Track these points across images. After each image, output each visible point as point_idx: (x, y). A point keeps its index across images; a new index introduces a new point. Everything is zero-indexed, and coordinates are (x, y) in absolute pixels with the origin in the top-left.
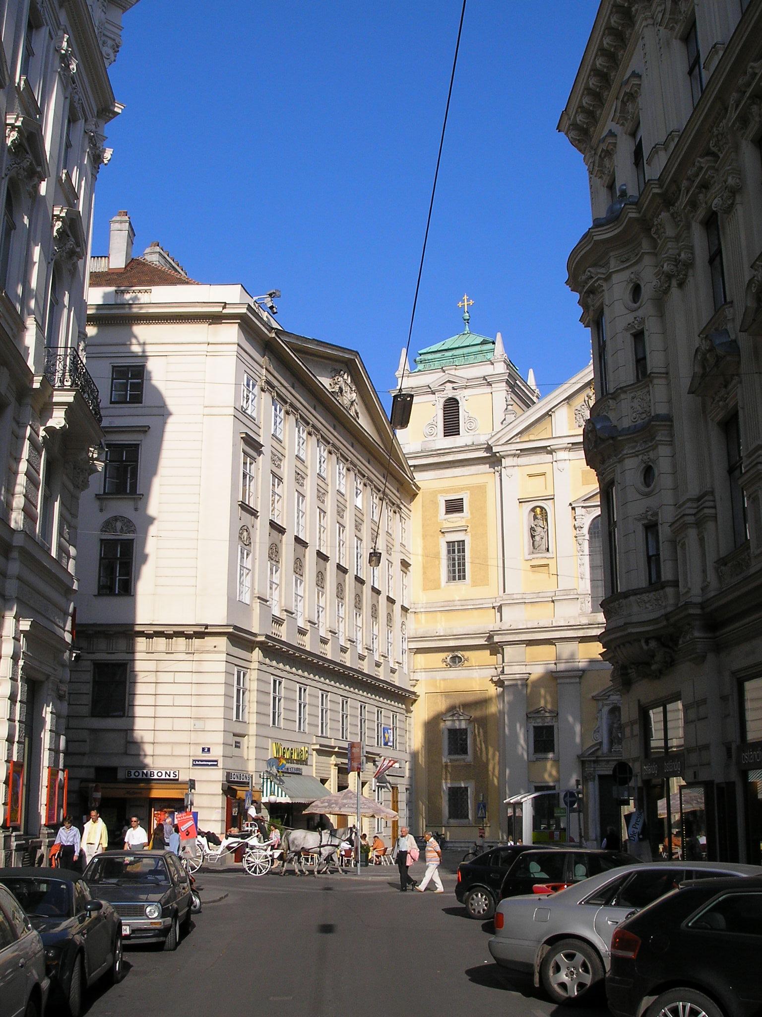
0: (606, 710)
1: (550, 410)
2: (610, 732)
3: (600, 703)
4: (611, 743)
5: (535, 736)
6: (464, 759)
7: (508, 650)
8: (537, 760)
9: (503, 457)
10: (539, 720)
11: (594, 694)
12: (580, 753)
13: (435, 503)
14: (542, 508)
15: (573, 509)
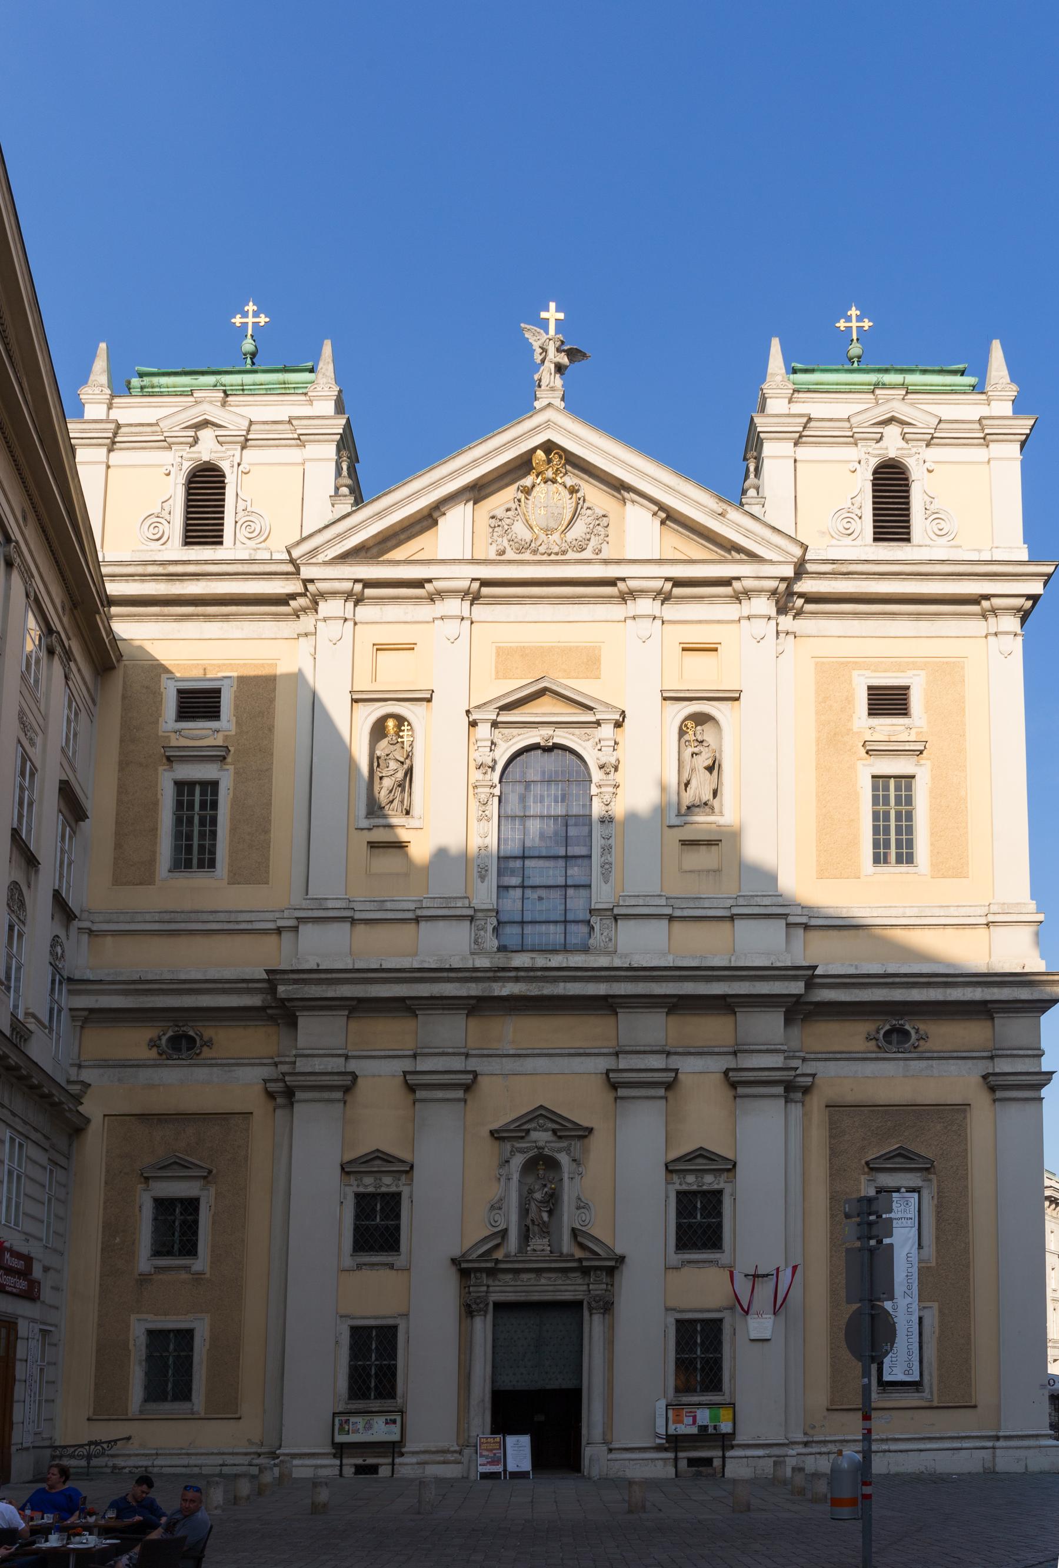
0: (518, 1160)
2: (524, 1212)
3: (508, 1146)
4: (525, 1236)
5: (357, 1217)
6: (187, 1268)
7: (305, 1022)
8: (360, 1267)
10: (368, 1180)
11: (495, 1126)
12: (457, 1253)
15: (473, 724)
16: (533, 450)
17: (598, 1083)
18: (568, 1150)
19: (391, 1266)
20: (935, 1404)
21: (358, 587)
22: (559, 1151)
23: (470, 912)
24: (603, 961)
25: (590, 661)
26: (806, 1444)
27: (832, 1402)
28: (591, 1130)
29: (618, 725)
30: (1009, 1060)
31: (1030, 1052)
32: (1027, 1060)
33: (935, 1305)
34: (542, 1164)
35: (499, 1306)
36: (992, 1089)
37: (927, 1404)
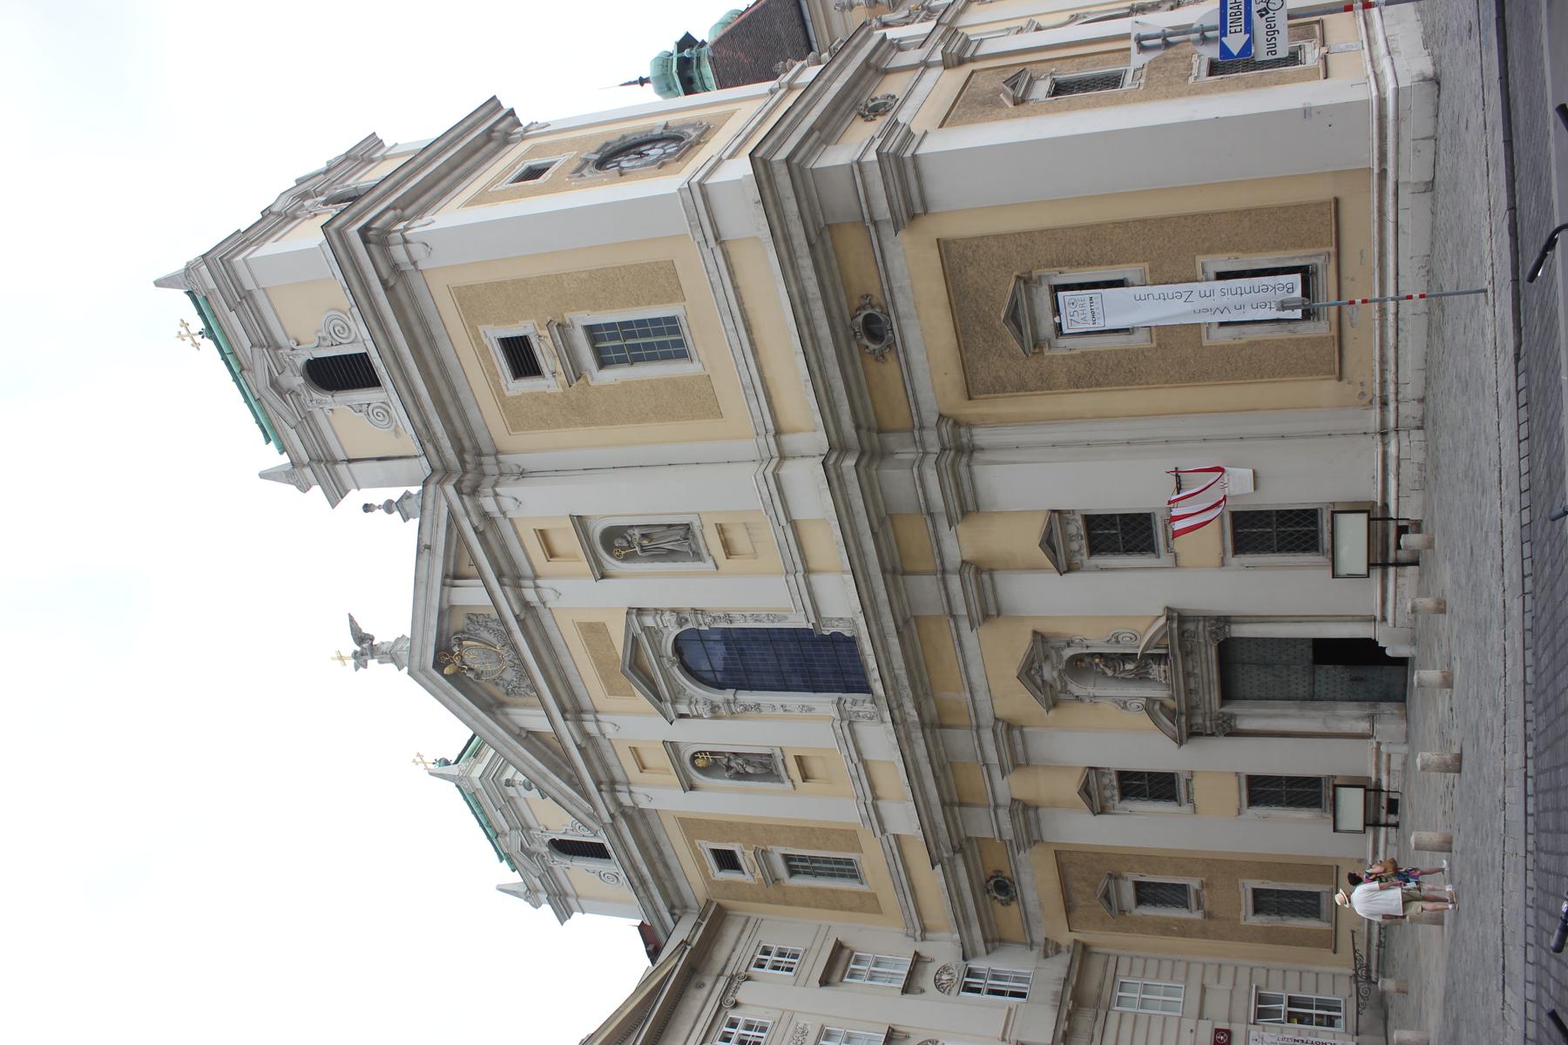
1: (517, 737)
8: (1190, 800)
9: (620, 805)
13: (728, 884)
14: (693, 758)
16: (445, 676)
17: (985, 631)
18: (1058, 650)
19: (1188, 782)
20: (1332, 249)
21: (603, 787)
22: (1061, 656)
23: (845, 724)
24: (861, 620)
25: (594, 632)
26: (1384, 404)
27: (1332, 372)
28: (1035, 633)
29: (640, 611)
30: (873, 202)
31: (858, 180)
32: (868, 180)
33: (1200, 259)
34: (1081, 665)
35: (1227, 695)
36: (912, 216)
37: (1333, 259)
